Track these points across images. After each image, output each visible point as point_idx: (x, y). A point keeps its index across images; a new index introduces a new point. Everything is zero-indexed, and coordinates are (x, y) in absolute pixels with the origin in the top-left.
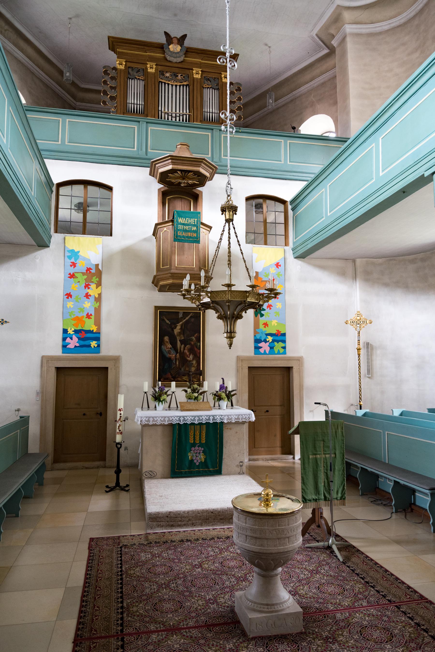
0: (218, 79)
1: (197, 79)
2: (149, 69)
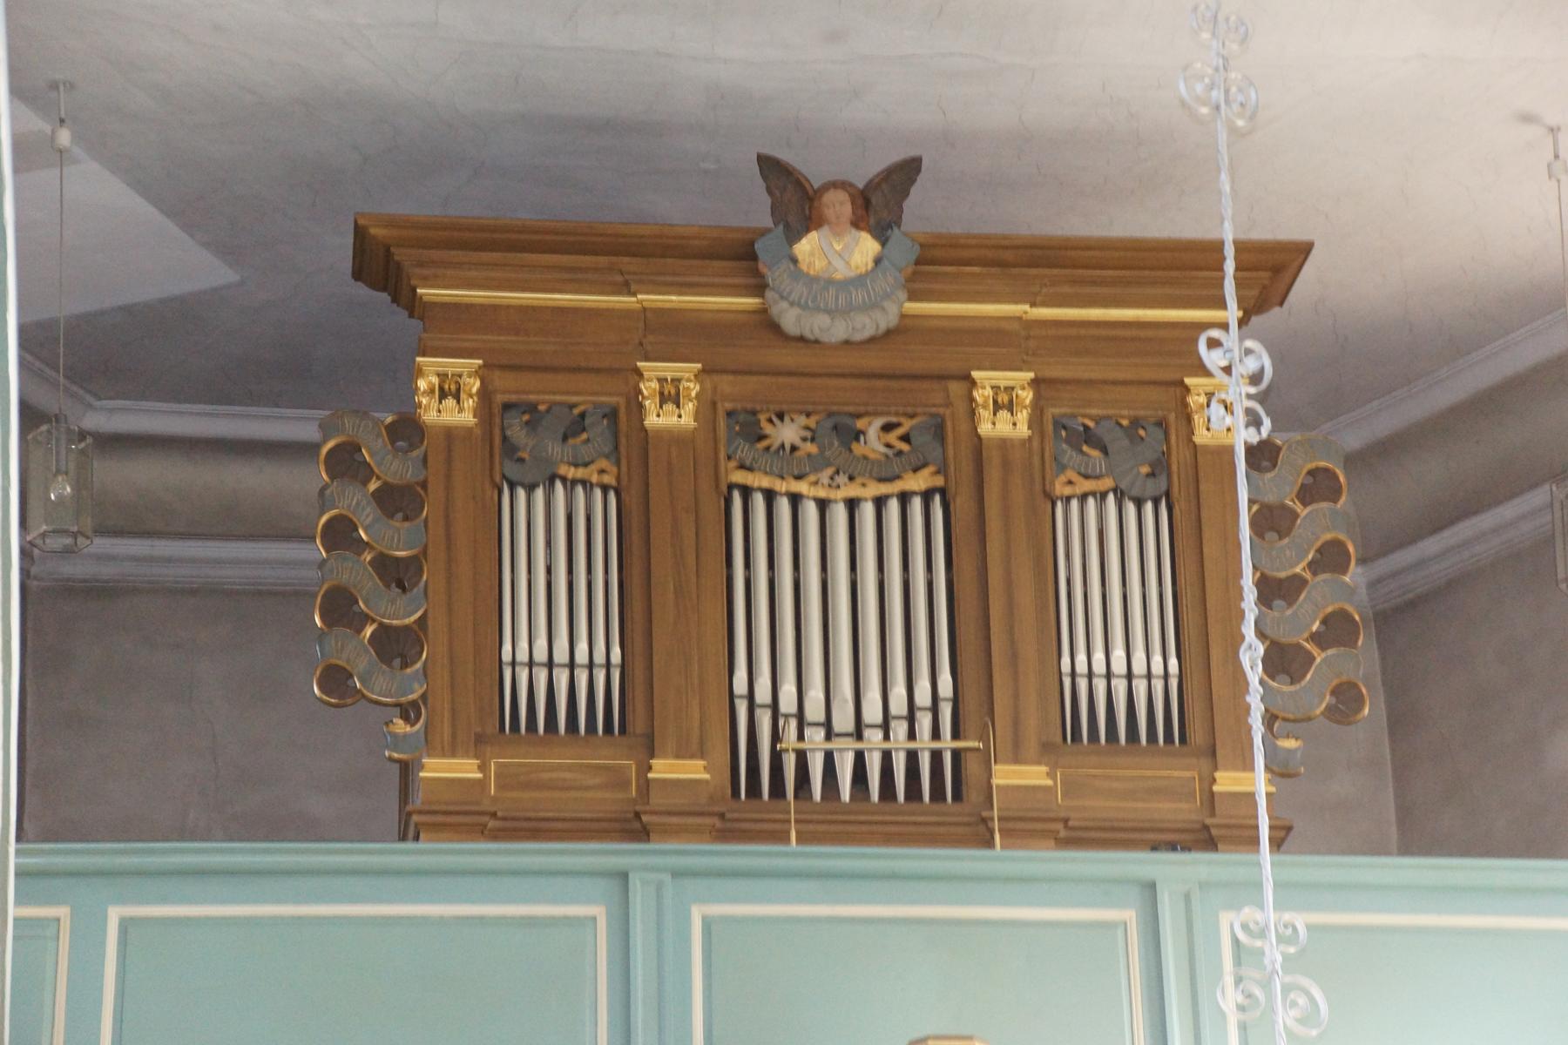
0: (1161, 424)
1: (1004, 444)
2: (650, 405)
